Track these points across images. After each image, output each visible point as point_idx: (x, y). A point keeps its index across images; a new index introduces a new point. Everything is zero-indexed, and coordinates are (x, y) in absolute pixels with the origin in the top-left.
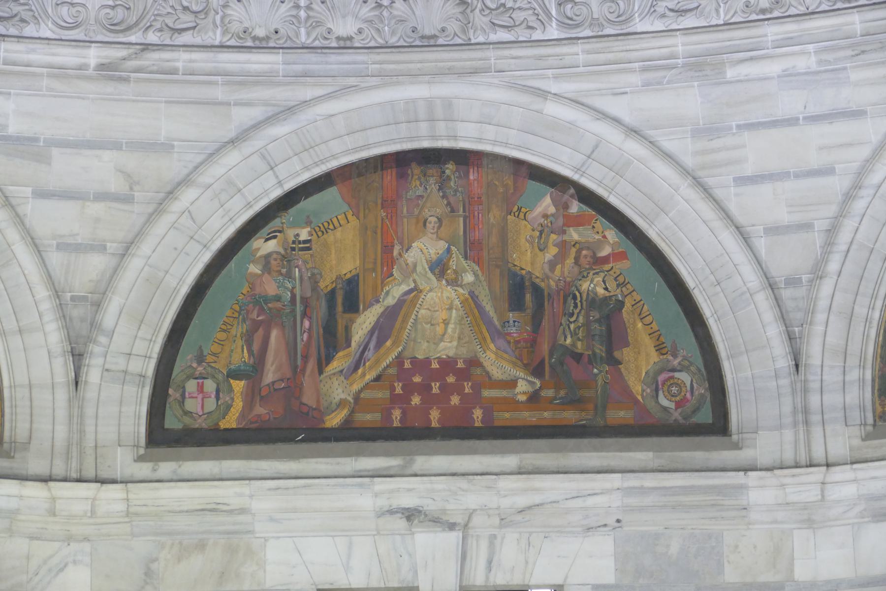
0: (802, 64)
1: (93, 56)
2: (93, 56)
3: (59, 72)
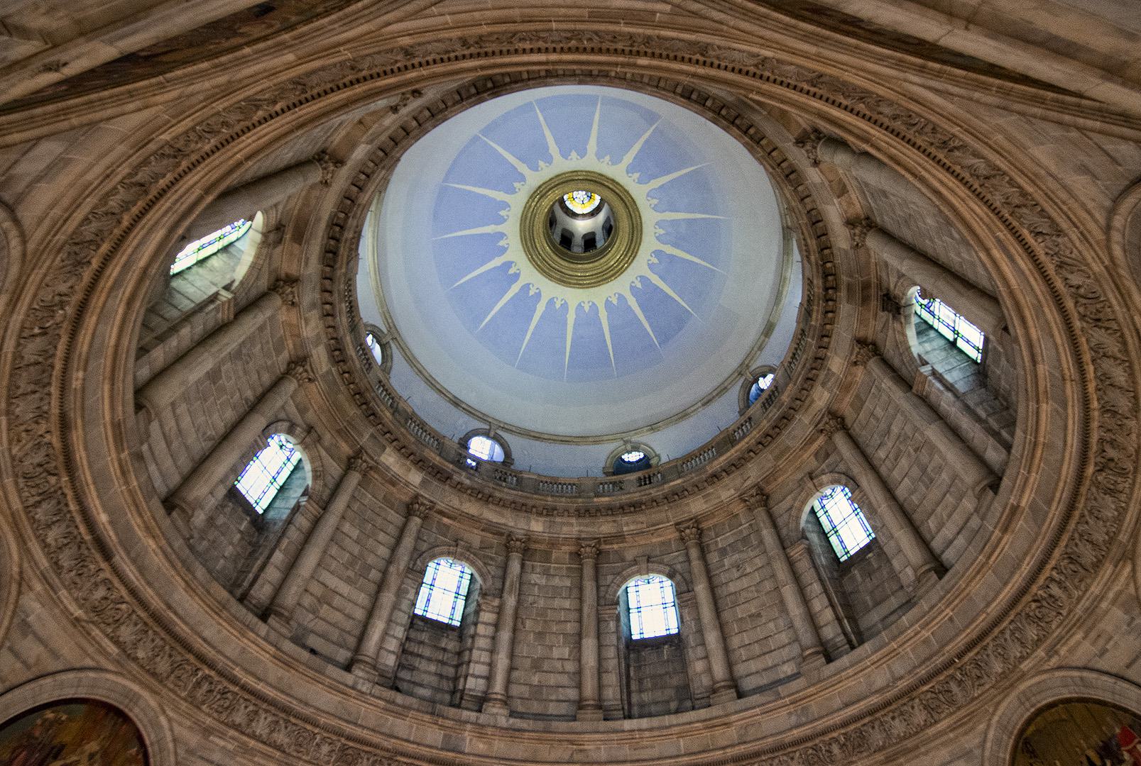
0: (230, 747)
1: (79, 613)
2: (79, 613)
3: (65, 611)
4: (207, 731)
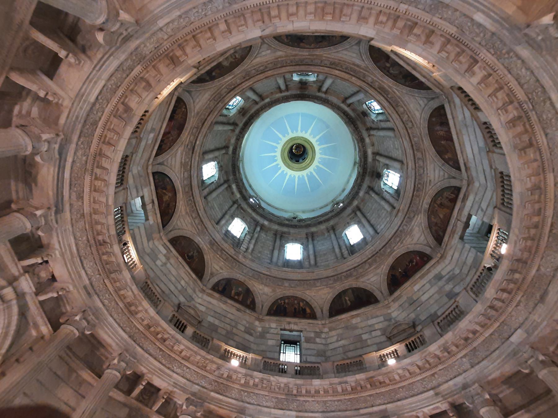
2: (183, 161)
4: (187, 213)
